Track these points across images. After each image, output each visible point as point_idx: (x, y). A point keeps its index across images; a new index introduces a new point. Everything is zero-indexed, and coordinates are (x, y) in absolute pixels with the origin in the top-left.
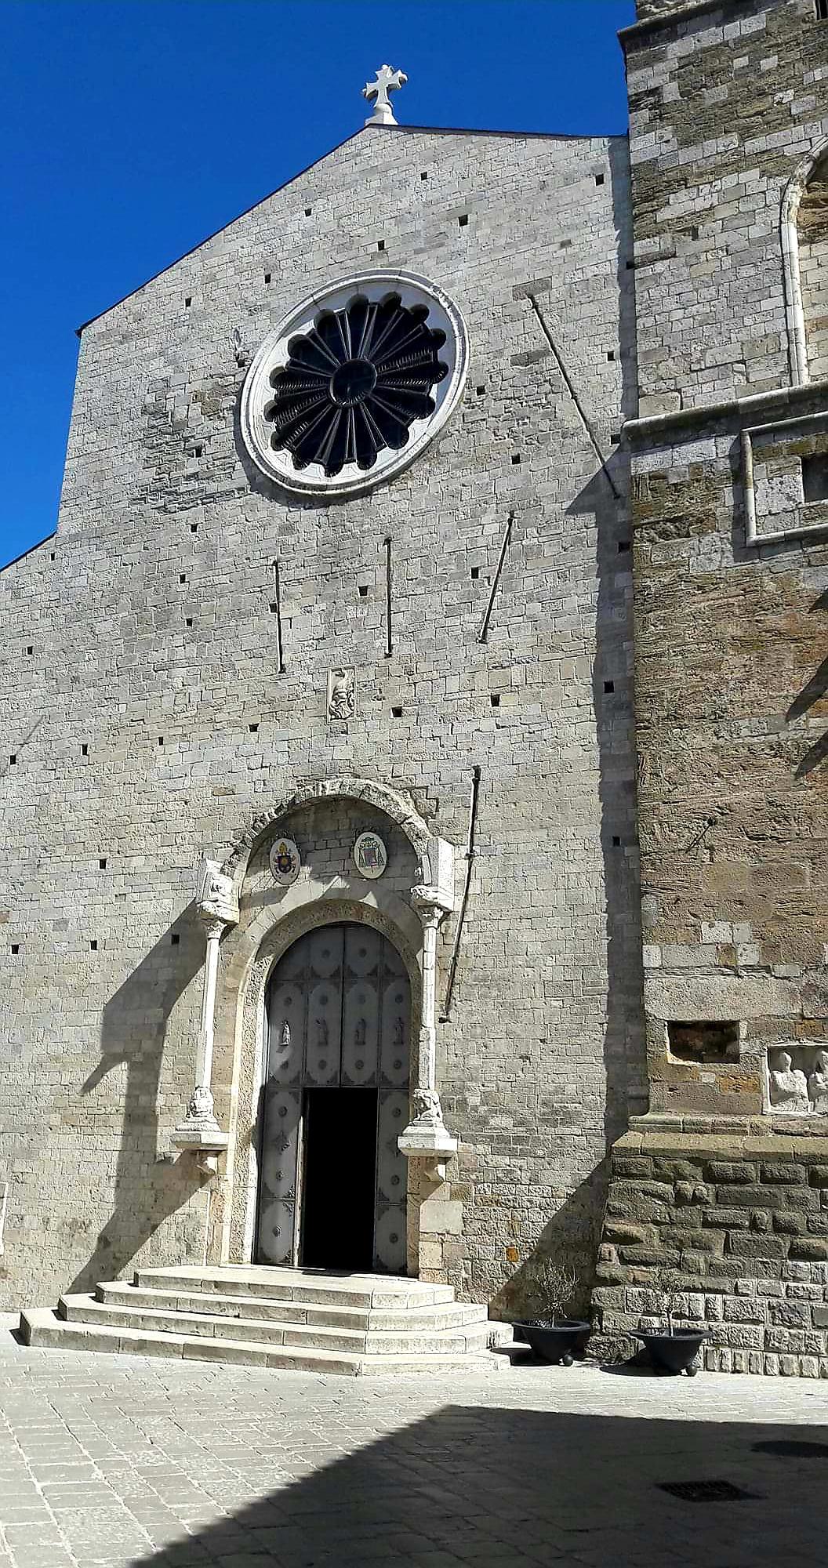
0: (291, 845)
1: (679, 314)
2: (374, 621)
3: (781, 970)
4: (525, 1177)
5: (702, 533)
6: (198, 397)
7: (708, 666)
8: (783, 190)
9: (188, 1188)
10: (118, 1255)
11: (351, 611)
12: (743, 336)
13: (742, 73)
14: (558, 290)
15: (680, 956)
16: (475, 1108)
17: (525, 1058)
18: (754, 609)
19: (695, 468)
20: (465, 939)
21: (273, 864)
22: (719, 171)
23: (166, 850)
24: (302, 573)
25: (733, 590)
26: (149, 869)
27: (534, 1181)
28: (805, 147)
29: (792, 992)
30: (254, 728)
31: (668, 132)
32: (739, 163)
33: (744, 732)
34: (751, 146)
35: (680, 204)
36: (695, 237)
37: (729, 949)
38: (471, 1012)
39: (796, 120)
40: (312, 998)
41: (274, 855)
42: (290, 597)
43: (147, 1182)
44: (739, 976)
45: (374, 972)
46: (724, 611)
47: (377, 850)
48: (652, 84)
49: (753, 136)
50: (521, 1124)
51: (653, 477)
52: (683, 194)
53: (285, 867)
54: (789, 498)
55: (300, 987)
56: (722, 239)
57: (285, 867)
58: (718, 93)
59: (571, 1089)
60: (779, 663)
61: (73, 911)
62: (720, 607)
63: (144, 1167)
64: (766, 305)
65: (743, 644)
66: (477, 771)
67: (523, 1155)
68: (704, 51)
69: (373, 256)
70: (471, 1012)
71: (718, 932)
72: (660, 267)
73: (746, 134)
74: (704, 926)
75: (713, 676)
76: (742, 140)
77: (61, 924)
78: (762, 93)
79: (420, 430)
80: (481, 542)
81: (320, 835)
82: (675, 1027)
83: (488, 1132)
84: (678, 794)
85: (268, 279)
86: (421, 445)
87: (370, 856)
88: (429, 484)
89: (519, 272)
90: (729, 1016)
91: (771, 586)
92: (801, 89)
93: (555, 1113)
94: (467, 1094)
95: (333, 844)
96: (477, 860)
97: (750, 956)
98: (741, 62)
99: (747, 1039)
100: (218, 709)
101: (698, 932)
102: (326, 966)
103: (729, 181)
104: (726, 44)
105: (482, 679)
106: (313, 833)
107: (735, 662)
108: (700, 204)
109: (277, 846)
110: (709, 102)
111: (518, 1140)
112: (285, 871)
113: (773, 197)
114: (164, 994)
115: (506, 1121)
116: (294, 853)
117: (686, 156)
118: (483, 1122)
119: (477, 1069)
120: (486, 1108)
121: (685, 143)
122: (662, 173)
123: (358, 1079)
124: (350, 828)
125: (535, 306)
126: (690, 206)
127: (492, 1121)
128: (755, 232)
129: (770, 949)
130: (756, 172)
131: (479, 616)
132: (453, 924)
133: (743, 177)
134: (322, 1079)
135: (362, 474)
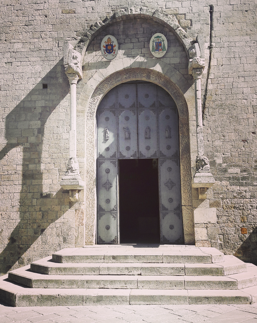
0: (113, 39)
4: (248, 195)
9: (62, 209)
10: (21, 246)
16: (220, 165)
17: (244, 141)
21: (103, 48)
23: (36, 40)
26: (25, 50)
38: (215, 121)
40: (120, 117)
41: (103, 44)
43: (37, 208)
45: (153, 105)
47: (162, 43)
50: (245, 171)
53: (110, 50)
55: (114, 112)
57: (110, 50)
63: (35, 201)
66: (211, 7)
67: (247, 185)
81: (127, 36)
83: (228, 176)
87: (158, 47)
94: (215, 159)
95: (134, 40)
96: (214, 50)
106: (123, 34)
109: (106, 39)
111: (244, 178)
112: (110, 53)
114: (41, 114)
115: (238, 170)
116: (115, 43)
118: (225, 171)
119: (220, 147)
120: (226, 164)
123: (147, 155)
124: (144, 33)
127: (229, 170)
134: (128, 155)
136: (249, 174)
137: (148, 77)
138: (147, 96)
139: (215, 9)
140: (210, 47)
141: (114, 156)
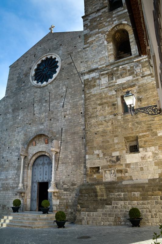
1: (90, 55)
2: (47, 106)
3: (106, 157)
5: (94, 88)
6: (24, 74)
7: (95, 108)
8: (104, 36)
11: (44, 104)
12: (100, 57)
13: (98, 21)
14: (74, 53)
15: (91, 156)
17: (69, 175)
18: (101, 99)
19: (93, 78)
20: (60, 156)
22: (96, 34)
24: (37, 99)
25: (98, 96)
27: (70, 195)
28: (107, 30)
29: (107, 161)
30: (30, 124)
31: (88, 30)
32: (98, 33)
33: (100, 119)
34: (100, 30)
35: (90, 40)
36: (93, 44)
37: (98, 155)
38: (61, 168)
39: (107, 26)
42: (35, 103)
44: (100, 159)
46: (97, 99)
48: (86, 23)
49: (100, 29)
50: (68, 186)
51: (87, 79)
52: (91, 38)
54: (106, 81)
56: (96, 44)
58: (96, 24)
59: (75, 180)
60: (105, 107)
61: (4, 156)
62: (97, 99)
64: (102, 53)
65: (100, 105)
68: (93, 18)
69: (49, 51)
70: (61, 168)
71: (96, 152)
72: (88, 49)
73: (99, 30)
74: (95, 151)
75: (96, 110)
76: (99, 30)
77: (3, 158)
78: (101, 23)
79: (55, 76)
80: (63, 92)
82: (90, 168)
84: (91, 130)
85: (34, 56)
86: (54, 78)
88: (55, 84)
89: (69, 51)
90: (98, 166)
91: (104, 95)
92: (106, 22)
93: (73, 184)
95: (41, 142)
97: (101, 155)
98: (99, 19)
99: (101, 169)
100: (25, 122)
101: (94, 152)
102: (41, 163)
103: (97, 35)
104: (96, 17)
105: (63, 114)
107: (99, 107)
108: (93, 39)
110: (94, 25)
111: (68, 189)
113: (103, 37)
117: (91, 33)
118: (63, 186)
121: (91, 31)
122: (88, 36)
123: (46, 180)
125: (71, 56)
126: (92, 40)
128: (101, 42)
129: (104, 155)
130: (101, 34)
131: (62, 103)
132: (58, 154)
133: (99, 35)
134: (40, 181)
135: (46, 83)
136: (70, 187)
137: (45, 153)
138: (46, 160)
139: (63, 129)
140: (61, 142)
141: (37, 181)
